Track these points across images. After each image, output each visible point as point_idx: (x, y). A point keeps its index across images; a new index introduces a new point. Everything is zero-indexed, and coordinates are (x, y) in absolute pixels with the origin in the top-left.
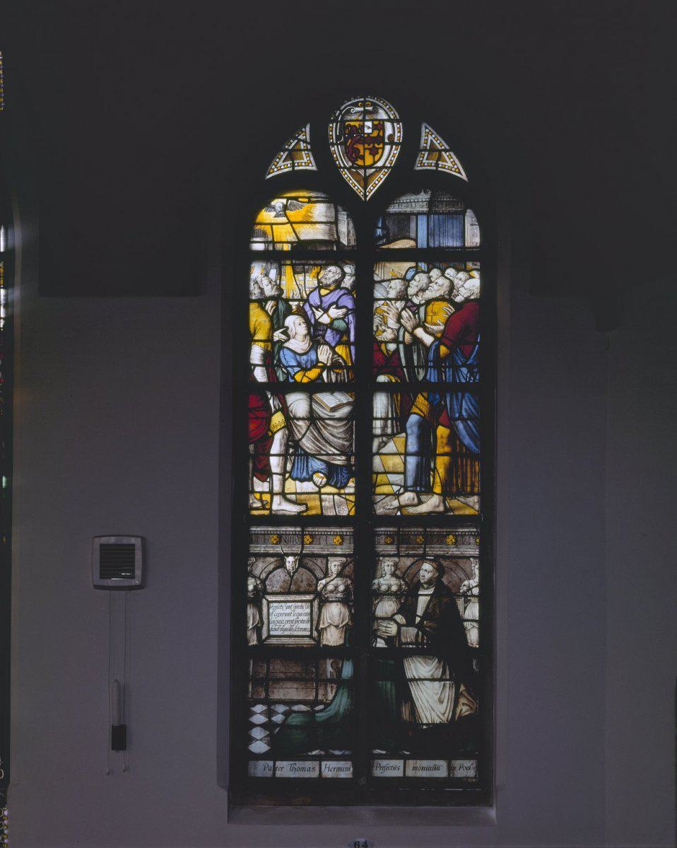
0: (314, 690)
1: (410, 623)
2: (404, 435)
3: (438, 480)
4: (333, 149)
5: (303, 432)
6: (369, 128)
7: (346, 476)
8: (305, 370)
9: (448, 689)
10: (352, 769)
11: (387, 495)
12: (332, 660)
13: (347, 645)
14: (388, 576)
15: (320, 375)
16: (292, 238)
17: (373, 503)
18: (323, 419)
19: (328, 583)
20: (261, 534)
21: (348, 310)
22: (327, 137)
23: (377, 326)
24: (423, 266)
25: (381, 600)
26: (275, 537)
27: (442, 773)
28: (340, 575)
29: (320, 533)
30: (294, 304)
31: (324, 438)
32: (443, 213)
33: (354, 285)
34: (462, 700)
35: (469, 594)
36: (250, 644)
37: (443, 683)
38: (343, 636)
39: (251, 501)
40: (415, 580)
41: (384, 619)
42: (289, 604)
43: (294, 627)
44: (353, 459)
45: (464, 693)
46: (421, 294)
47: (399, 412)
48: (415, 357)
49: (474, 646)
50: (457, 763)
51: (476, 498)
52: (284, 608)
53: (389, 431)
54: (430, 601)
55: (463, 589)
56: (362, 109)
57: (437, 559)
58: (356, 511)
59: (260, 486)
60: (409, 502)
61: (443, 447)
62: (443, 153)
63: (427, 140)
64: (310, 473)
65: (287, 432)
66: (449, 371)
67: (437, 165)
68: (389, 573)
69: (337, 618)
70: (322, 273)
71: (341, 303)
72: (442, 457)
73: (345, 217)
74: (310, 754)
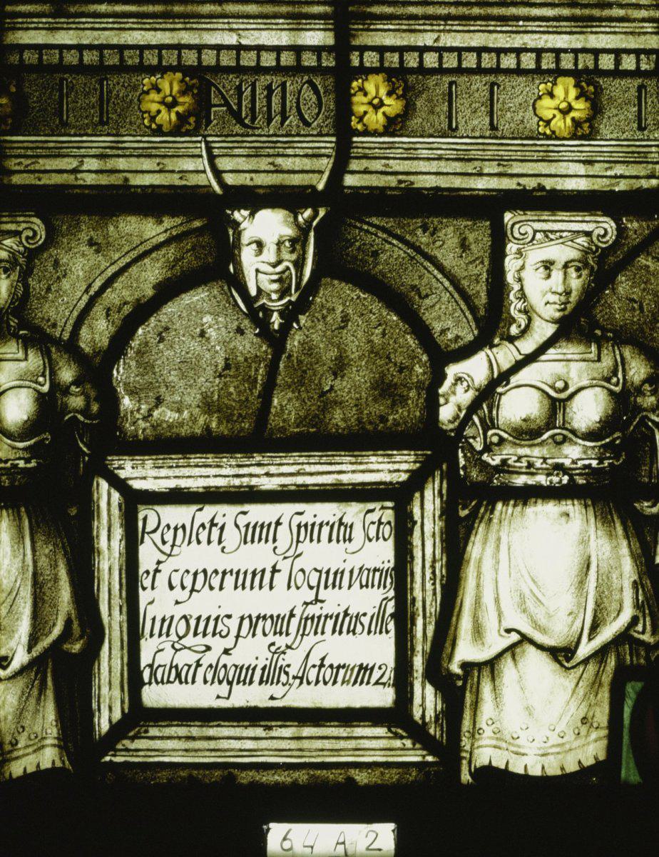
13: (629, 772)
19: (505, 377)
20: (81, 68)
26: (170, 84)
29: (451, 61)
36: (17, 769)
38: (602, 715)
42: (260, 513)
43: (294, 660)
52: (232, 536)
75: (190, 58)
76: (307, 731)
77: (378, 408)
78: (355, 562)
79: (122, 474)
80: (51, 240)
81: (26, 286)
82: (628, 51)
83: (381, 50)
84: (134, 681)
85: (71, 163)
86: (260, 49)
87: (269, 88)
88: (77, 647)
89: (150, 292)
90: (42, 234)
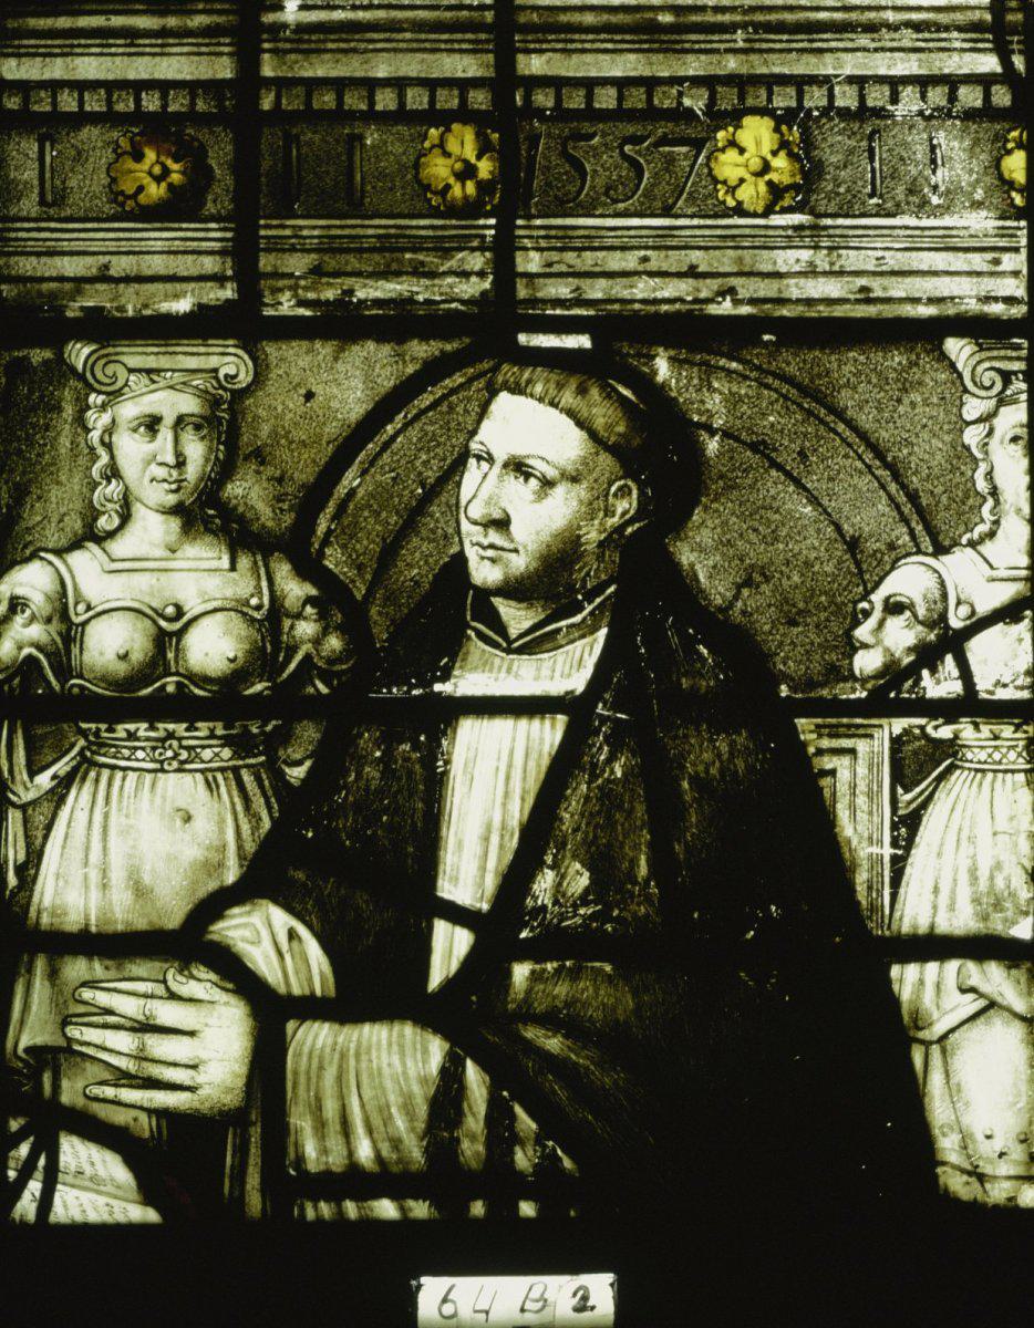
14: (150, 530)
25: (85, 765)
40: (417, 564)
49: (998, 1193)
68: (165, 497)
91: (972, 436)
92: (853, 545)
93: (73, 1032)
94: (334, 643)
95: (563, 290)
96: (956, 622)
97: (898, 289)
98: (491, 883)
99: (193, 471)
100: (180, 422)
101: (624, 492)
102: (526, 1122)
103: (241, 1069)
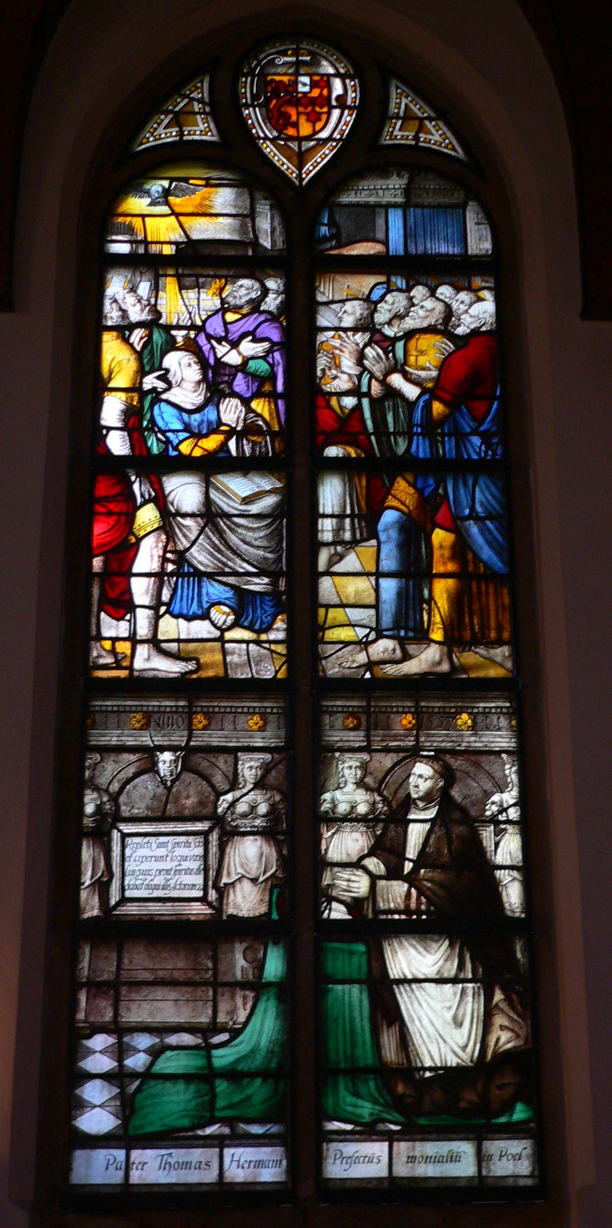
0: (210, 1003)
1: (394, 873)
2: (374, 542)
3: (437, 619)
4: (247, 112)
5: (193, 538)
6: (304, 84)
7: (270, 611)
8: (197, 436)
9: (470, 999)
10: (284, 1162)
11: (346, 644)
12: (244, 945)
13: (275, 916)
14: (350, 787)
15: (224, 446)
16: (178, 236)
17: (317, 659)
18: (229, 516)
19: (238, 800)
20: (112, 712)
21: (273, 344)
22: (235, 96)
23: (323, 370)
24: (400, 282)
25: (337, 831)
26: (139, 716)
27: (466, 1168)
28: (259, 784)
29: (222, 710)
30: (179, 335)
31: (230, 548)
32: (429, 206)
33: (284, 308)
34: (499, 1020)
35: (502, 818)
36: (86, 916)
37: (460, 986)
38: (267, 898)
39: (95, 654)
40: (401, 794)
41: (344, 865)
43: (172, 883)
44: (282, 583)
45: (503, 1005)
46: (398, 323)
47: (363, 504)
48: (390, 418)
49: (517, 915)
50: (494, 1147)
51: (505, 650)
53: (347, 536)
54: (430, 832)
55: (493, 809)
56: (294, 59)
57: (439, 757)
58: (288, 670)
59: (111, 628)
60: (386, 656)
61: (444, 563)
62: (427, 122)
63: (400, 104)
64: (205, 606)
65: (164, 537)
66: (450, 440)
67: (416, 138)
69: (255, 865)
70: (228, 288)
71: (261, 332)
72: (443, 580)
73: (268, 207)
74: (200, 1132)
75: (145, 709)
76: (176, 904)
77: (199, 809)
78: (191, 853)
79: (121, 828)
80: (102, 760)
81: (94, 774)
82: (275, 707)
83: (202, 707)
84: (123, 889)
85: (109, 738)
86: (166, 706)
87: (169, 718)
88: (105, 879)
89: (131, 775)
90: (99, 759)
91: (507, 772)
92: (485, 791)
93: (335, 881)
94: (386, 808)
95: (429, 744)
96: (505, 806)
97: (493, 745)
98: (416, 854)
99: (358, 776)
100: (356, 767)
101: (441, 781)
102: (423, 900)
103: (368, 889)
